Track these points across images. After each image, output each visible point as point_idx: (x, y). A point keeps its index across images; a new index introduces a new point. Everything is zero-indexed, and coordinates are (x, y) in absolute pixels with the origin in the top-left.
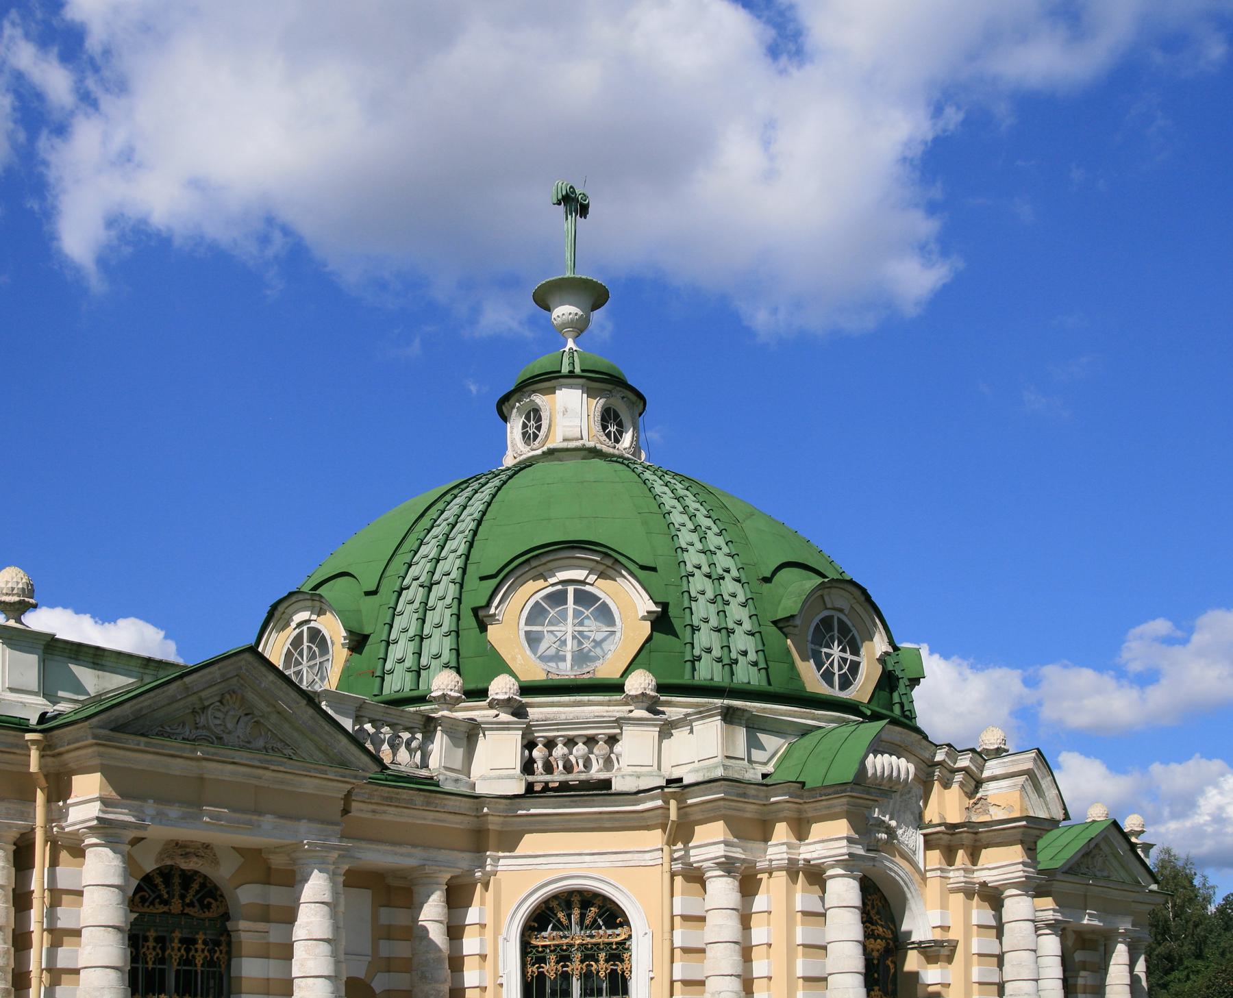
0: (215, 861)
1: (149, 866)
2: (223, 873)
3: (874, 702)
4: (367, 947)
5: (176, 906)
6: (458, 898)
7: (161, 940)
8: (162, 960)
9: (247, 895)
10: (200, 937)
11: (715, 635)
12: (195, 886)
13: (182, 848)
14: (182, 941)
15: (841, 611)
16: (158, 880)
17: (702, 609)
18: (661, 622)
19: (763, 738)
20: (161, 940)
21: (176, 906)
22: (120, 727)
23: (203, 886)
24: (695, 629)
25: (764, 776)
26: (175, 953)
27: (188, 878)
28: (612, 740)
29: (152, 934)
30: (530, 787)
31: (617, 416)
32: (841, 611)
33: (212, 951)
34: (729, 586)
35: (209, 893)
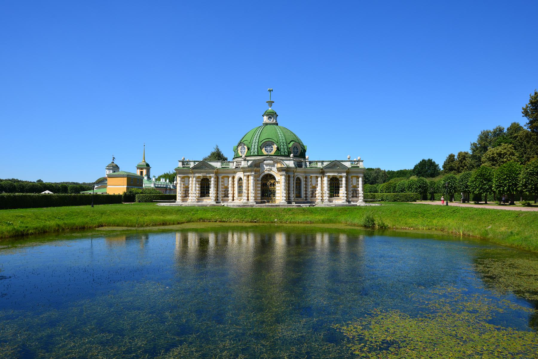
1: (202, 178)
2: (208, 178)
3: (275, 153)
5: (205, 181)
6: (233, 178)
9: (210, 180)
13: (204, 176)
18: (248, 149)
19: (249, 161)
20: (204, 184)
21: (205, 181)
22: (193, 169)
24: (251, 149)
25: (248, 166)
27: (206, 178)
28: (241, 162)
34: (256, 144)
35: (208, 180)
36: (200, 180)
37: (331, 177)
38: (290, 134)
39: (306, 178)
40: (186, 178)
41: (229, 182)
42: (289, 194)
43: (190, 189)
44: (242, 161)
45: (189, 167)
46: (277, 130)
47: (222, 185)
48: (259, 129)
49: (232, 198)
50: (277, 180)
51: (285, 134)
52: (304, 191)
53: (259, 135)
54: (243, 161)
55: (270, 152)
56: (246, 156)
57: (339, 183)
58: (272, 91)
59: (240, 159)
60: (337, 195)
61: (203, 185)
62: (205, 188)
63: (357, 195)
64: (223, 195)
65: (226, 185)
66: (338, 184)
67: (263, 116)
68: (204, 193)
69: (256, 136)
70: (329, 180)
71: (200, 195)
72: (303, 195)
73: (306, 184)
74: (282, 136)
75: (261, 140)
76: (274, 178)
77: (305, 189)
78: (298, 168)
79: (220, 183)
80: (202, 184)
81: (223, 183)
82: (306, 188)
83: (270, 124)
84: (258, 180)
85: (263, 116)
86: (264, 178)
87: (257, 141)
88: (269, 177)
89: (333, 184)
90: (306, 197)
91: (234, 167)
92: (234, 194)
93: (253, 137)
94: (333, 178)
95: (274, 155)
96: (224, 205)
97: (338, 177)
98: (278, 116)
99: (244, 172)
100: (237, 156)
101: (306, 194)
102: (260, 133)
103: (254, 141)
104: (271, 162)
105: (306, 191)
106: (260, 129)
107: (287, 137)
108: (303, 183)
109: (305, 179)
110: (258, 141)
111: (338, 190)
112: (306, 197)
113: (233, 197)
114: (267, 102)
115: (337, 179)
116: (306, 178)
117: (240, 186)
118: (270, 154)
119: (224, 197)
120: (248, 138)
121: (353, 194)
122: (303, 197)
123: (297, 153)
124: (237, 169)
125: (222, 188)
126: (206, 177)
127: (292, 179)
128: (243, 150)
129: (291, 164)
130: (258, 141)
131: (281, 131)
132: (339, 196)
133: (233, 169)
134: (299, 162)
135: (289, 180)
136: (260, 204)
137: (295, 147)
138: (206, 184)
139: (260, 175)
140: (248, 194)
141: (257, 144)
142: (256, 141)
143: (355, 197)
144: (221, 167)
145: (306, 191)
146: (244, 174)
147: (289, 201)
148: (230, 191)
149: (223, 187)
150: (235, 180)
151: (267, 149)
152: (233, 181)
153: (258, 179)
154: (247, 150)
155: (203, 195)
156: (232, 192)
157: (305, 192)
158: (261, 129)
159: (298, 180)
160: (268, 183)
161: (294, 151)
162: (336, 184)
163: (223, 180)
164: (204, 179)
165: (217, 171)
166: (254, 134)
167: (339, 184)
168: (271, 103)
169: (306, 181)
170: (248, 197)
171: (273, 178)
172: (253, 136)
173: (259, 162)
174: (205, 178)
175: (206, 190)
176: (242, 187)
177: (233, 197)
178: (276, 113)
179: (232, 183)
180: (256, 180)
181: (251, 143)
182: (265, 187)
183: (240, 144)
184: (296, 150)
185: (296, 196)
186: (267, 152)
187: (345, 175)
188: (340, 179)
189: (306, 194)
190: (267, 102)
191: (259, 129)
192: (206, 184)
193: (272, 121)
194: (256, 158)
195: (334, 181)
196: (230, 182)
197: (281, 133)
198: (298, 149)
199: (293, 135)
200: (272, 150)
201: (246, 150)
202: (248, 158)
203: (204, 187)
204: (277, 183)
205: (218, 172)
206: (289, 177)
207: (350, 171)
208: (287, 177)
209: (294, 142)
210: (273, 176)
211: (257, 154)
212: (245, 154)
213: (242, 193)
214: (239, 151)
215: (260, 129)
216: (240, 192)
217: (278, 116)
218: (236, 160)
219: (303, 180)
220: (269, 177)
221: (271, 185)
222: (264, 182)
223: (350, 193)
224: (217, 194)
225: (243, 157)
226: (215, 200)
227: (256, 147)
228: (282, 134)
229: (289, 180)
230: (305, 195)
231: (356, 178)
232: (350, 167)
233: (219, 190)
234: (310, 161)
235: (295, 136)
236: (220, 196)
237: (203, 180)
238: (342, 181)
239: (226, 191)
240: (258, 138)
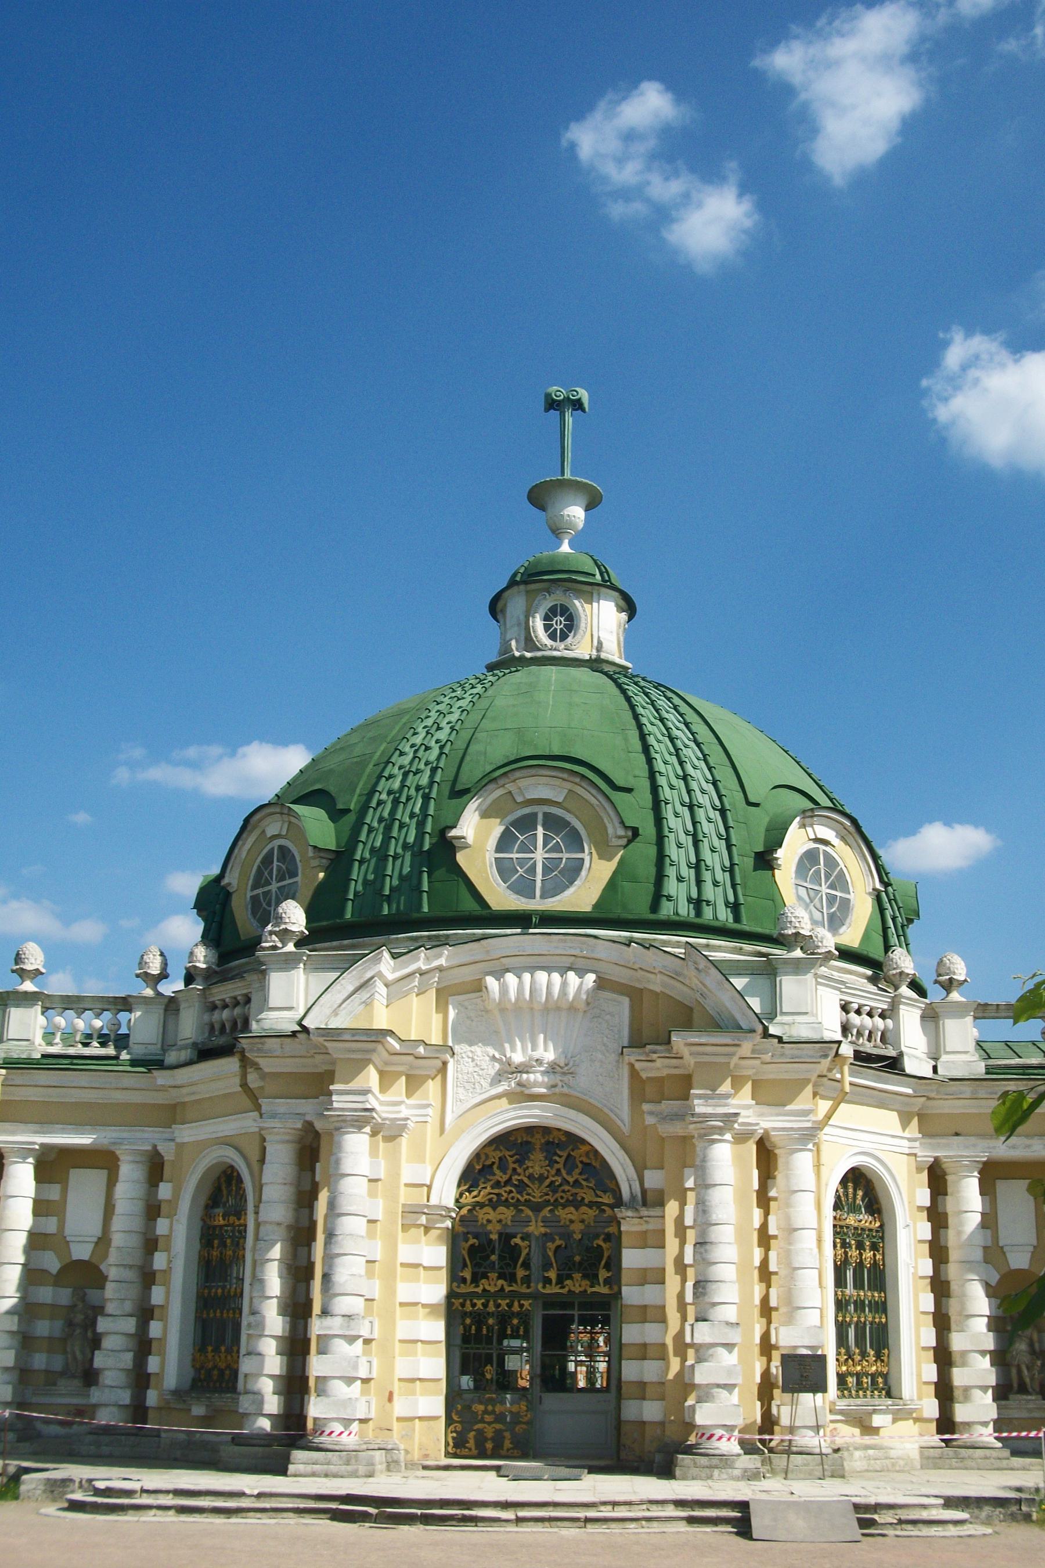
149: (52, 1263)
163: (53, 1192)
182: (493, 1284)
220: (537, 1164)
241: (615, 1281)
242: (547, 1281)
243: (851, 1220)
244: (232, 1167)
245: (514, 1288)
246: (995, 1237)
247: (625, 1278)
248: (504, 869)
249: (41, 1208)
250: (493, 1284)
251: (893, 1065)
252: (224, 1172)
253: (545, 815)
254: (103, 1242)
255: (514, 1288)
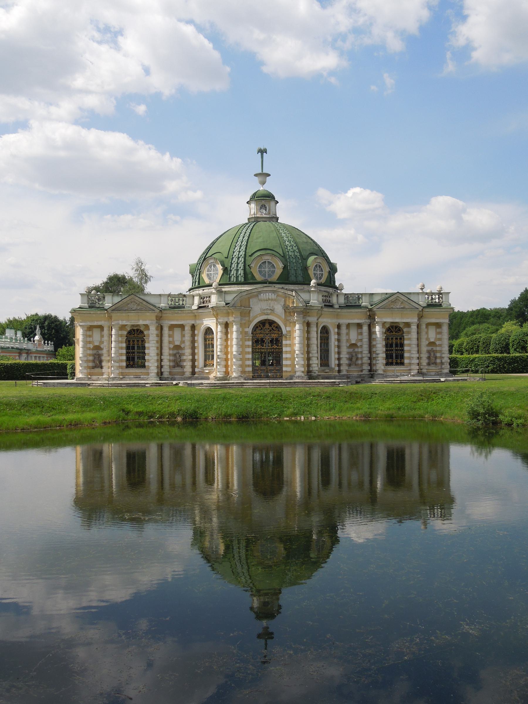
0: (140, 327)
1: (129, 329)
2: (142, 329)
4: (180, 339)
6: (193, 327)
7: (133, 341)
8: (134, 344)
10: (131, 340)
11: (242, 271)
12: (139, 331)
13: (133, 326)
14: (137, 341)
15: (268, 259)
16: (136, 331)
17: (234, 265)
20: (133, 341)
21: (136, 335)
23: (140, 331)
24: (230, 270)
26: (136, 342)
27: (138, 330)
28: (209, 297)
29: (131, 340)
30: (200, 308)
31: (265, 206)
32: (268, 259)
33: (142, 342)
34: (240, 259)
35: (142, 332)
36: (125, 333)
37: (388, 326)
38: (305, 240)
39: (339, 326)
40: (95, 330)
41: (183, 336)
42: (309, 359)
43: (104, 351)
44: (212, 293)
45: (104, 307)
46: (281, 231)
47: (170, 342)
48: (244, 231)
49: (191, 370)
50: (284, 332)
51: (298, 240)
52: (335, 354)
53: (244, 243)
54: (213, 293)
55: (270, 276)
56: (220, 285)
57: (403, 336)
58: (266, 152)
59: (207, 290)
60: (399, 361)
61: (131, 343)
62: (392, 347)
63: (438, 361)
64: (172, 364)
65: (177, 343)
66: (401, 339)
67: (247, 203)
68: (133, 359)
69: (239, 243)
70: (384, 330)
71: (124, 364)
72: (333, 362)
73: (339, 340)
74: (292, 243)
75: (249, 252)
76: (278, 328)
77: (336, 350)
78: (326, 309)
79: (166, 339)
80: (129, 341)
81: (171, 339)
82: (339, 347)
83: (265, 220)
84: (246, 333)
85: (247, 203)
86: (257, 327)
87: (242, 253)
88: (267, 326)
89: (392, 339)
90: (339, 365)
91: (195, 307)
92: (193, 361)
93: (233, 246)
94: (392, 327)
95: (277, 282)
96: (177, 384)
97: (401, 326)
98: (278, 202)
99: (216, 316)
100: (199, 284)
101: (339, 359)
102: (246, 238)
103: (235, 254)
104: (272, 296)
105: (339, 353)
106: (245, 229)
107: (301, 246)
108: (333, 337)
109: (336, 330)
110: (244, 253)
111: (400, 350)
112: (339, 365)
113: (193, 367)
114: (256, 175)
115: (400, 330)
116: (339, 326)
117: (208, 345)
118: (270, 280)
119: (174, 367)
120: (223, 247)
121: (429, 358)
122: (333, 366)
123: (320, 278)
124: (201, 310)
125: (170, 349)
126: (138, 328)
127: (314, 329)
128: (212, 272)
129: (315, 300)
130: (245, 255)
131: (288, 235)
132: (402, 364)
133: (192, 311)
134: (325, 296)
135: (308, 332)
136: (251, 380)
137: (317, 265)
138: (138, 341)
139: (250, 322)
140: (227, 360)
141: (242, 259)
142: (241, 254)
143: (433, 364)
144: (168, 308)
145: (339, 353)
146: (217, 320)
147: (309, 374)
148: (187, 357)
149: (172, 346)
150: (196, 332)
151: (264, 271)
152: (193, 335)
153: (247, 330)
154: (222, 272)
155: (131, 363)
156: (190, 357)
157: (337, 356)
158: (249, 231)
159: (325, 331)
160: (267, 338)
161: (315, 274)
162: (396, 339)
163: (171, 333)
164: (134, 330)
165: (160, 315)
166: (235, 241)
167: (404, 340)
168: (263, 176)
169: (339, 334)
170: (226, 366)
171: (276, 327)
172: (234, 244)
173: (249, 296)
174: (135, 328)
175: (138, 352)
176: (213, 347)
177: (193, 367)
178: (273, 198)
179: (224, 338)
180: (242, 333)
181: (230, 257)
182: (259, 346)
183: (205, 258)
184: (318, 272)
185: (321, 364)
186: (264, 275)
187: (417, 321)
188: (405, 330)
189: (339, 359)
190: (256, 175)
191: (244, 231)
192: (138, 341)
193: (264, 214)
194: (240, 288)
195: (394, 333)
196: (188, 337)
197: (290, 239)
198: (322, 271)
199: (310, 241)
200: (273, 272)
201: (221, 272)
202: (226, 289)
203: (133, 348)
204: (284, 338)
205: (161, 317)
206: (308, 325)
207: (424, 313)
208: (305, 325)
209: (316, 256)
210: (275, 325)
211: (243, 280)
212: (218, 280)
213: (213, 358)
214: (204, 276)
215: (245, 229)
216: (209, 356)
217: (278, 202)
218: (200, 291)
219: (333, 331)
220: (267, 326)
221: (272, 341)
222: (260, 336)
223: (424, 356)
224: (161, 360)
225: (213, 285)
226: (157, 374)
227: (241, 265)
228: (292, 240)
229: (308, 332)
230: (337, 362)
231: (434, 327)
232: (425, 305)
233: (163, 354)
234: (346, 294)
235: (315, 245)
236: (166, 363)
237: (130, 333)
238: (409, 333)
239: (178, 356)
240: (243, 248)
241: (281, 346)
242: (269, 346)
243: (323, 335)
244: (209, 327)
245: (263, 347)
246: (349, 337)
247: (283, 346)
248: (260, 272)
249: (170, 336)
250: (259, 346)
251: (331, 306)
252: (208, 328)
253: (268, 261)
254: (183, 342)
255: (263, 347)
